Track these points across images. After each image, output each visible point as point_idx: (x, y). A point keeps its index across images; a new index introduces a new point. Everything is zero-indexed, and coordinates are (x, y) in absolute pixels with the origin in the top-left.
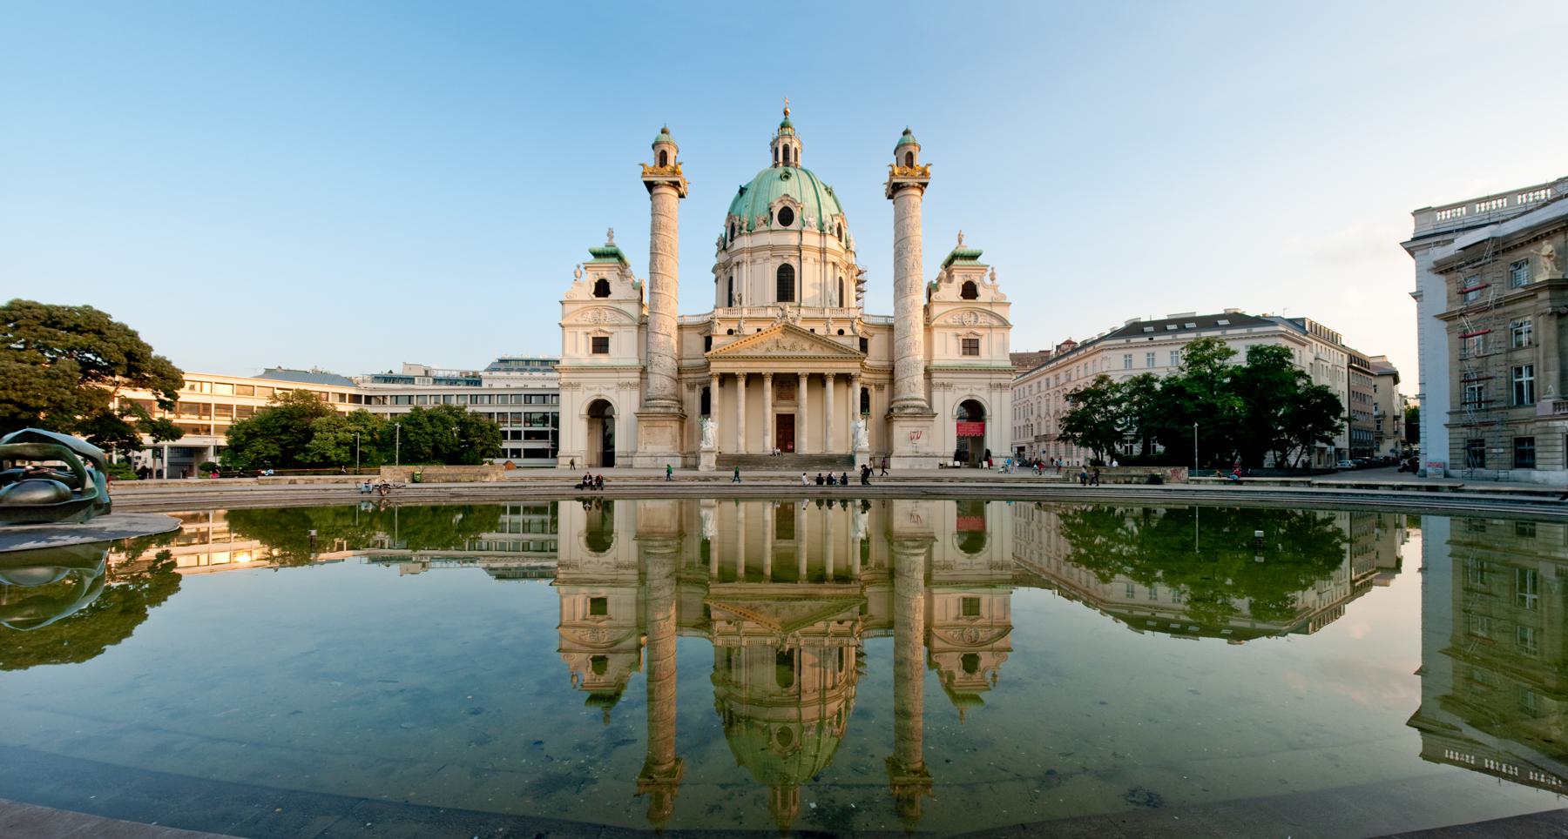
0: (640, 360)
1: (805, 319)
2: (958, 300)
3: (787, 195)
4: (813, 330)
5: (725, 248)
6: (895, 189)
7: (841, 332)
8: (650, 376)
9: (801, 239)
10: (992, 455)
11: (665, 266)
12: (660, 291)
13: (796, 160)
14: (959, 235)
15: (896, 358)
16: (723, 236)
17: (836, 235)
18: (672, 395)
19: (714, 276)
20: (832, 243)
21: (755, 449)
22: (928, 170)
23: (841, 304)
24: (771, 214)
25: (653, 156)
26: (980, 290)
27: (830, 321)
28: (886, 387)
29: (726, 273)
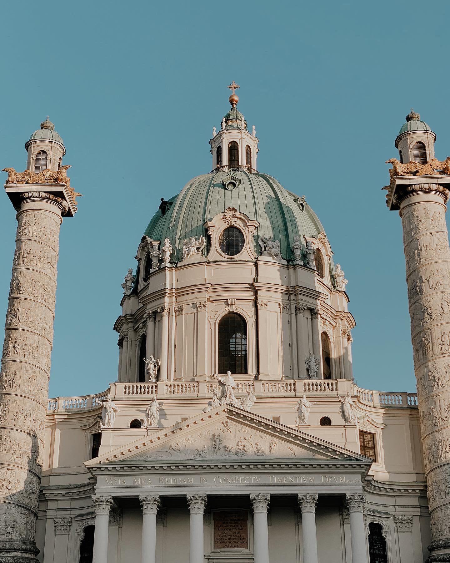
3: (234, 210)
5: (135, 292)
9: (257, 275)
11: (31, 318)
12: (21, 358)
13: (249, 161)
15: (428, 468)
16: (134, 273)
18: (24, 542)
19: (116, 336)
24: (209, 238)
27: (305, 401)
29: (136, 331)
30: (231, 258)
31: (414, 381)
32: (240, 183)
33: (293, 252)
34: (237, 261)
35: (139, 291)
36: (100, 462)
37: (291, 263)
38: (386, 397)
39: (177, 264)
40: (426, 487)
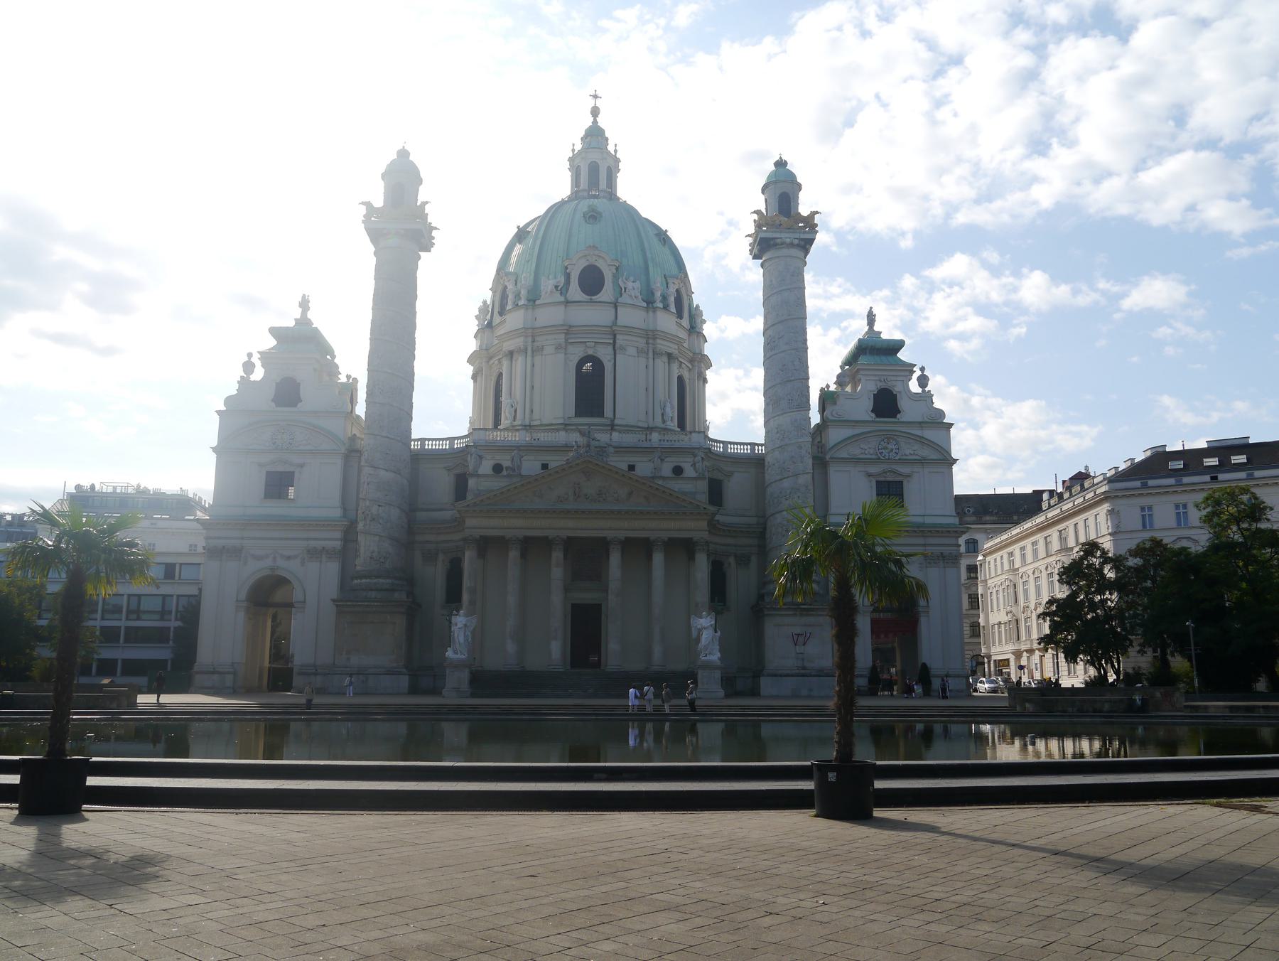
0: (345, 509)
1: (621, 450)
2: (870, 419)
3: (594, 247)
4: (632, 468)
5: (490, 325)
6: (762, 246)
7: (678, 471)
8: (361, 538)
9: (616, 318)
10: (933, 672)
14: (868, 316)
17: (673, 308)
19: (470, 370)
20: (666, 322)
21: (535, 662)
22: (817, 219)
23: (682, 424)
24: (568, 276)
25: (383, 191)
26: (903, 404)
28: (754, 559)
30: (591, 299)
31: (762, 432)
32: (601, 216)
33: (653, 294)
34: (596, 302)
35: (494, 324)
36: (468, 505)
37: (651, 305)
38: (736, 446)
39: (535, 301)
40: (765, 529)
